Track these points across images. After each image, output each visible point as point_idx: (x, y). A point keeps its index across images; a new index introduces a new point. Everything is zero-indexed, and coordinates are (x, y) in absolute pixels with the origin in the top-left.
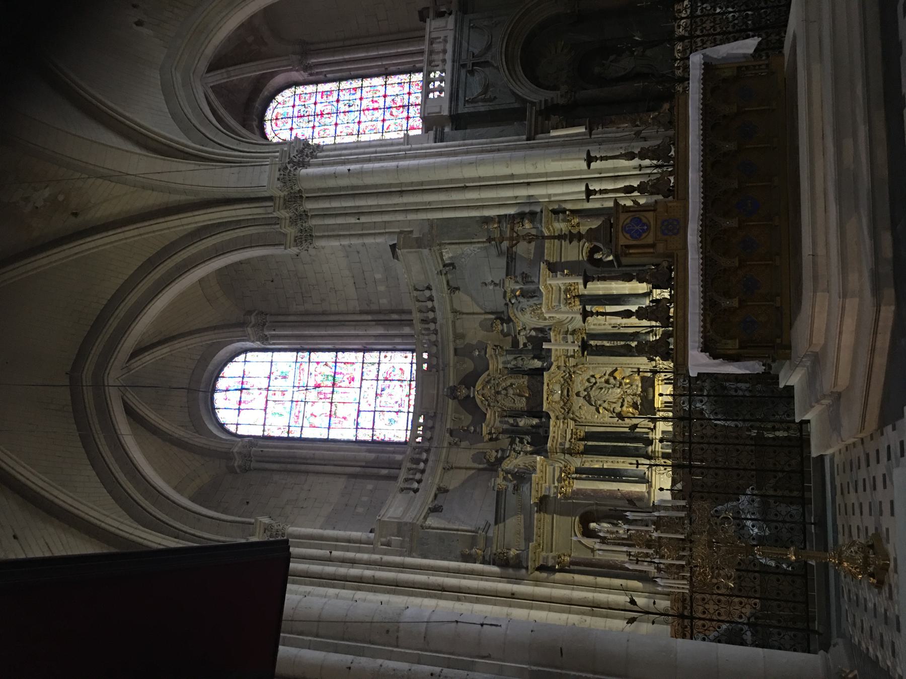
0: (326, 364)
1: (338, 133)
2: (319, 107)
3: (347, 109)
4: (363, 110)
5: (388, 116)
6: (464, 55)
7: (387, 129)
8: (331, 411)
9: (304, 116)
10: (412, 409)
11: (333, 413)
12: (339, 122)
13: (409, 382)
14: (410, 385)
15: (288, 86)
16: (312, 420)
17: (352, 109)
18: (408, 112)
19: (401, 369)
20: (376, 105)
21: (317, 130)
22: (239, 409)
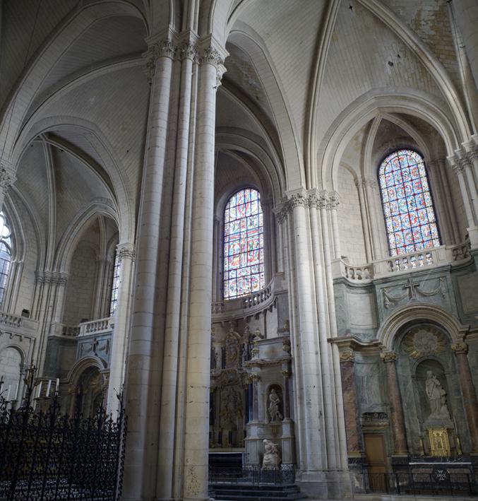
1: (392, 203)
3: (409, 203)
6: (415, 280)
12: (399, 201)
16: (232, 246)
17: (410, 206)
20: (413, 222)
21: (393, 188)
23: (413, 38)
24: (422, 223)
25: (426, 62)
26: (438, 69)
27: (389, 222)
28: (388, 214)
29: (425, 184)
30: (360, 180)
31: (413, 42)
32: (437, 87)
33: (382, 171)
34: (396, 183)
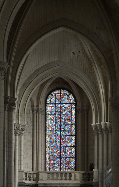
2: (64, 116)
4: (61, 137)
5: (57, 149)
7: (51, 149)
9: (61, 109)
15: (75, 100)
18: (58, 158)
20: (62, 143)
23: (90, 52)
24: (68, 145)
25: (94, 67)
26: (99, 74)
27: (48, 139)
28: (48, 133)
29: (73, 119)
30: (35, 108)
31: (90, 53)
32: (95, 78)
33: (48, 101)
34: (56, 113)
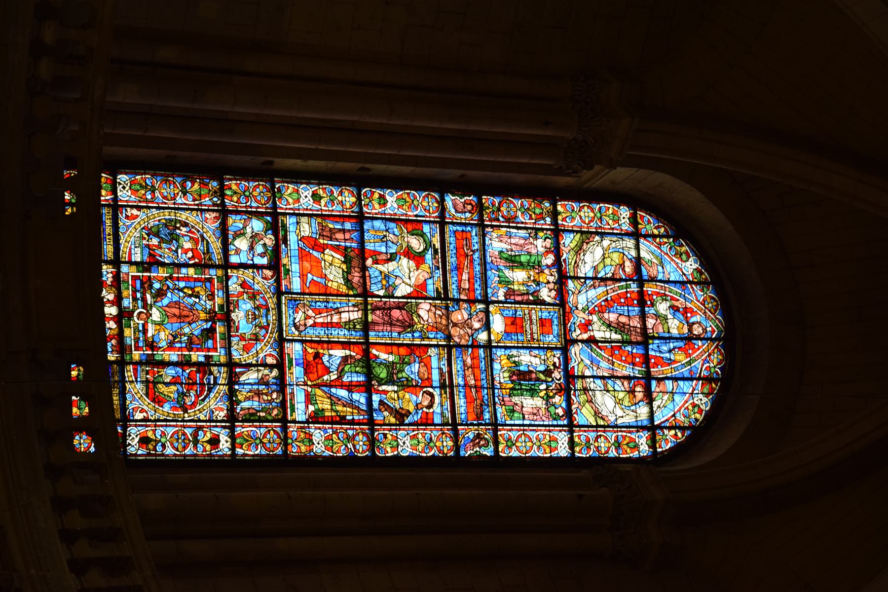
0: (401, 415)
8: (364, 269)
10: (107, 272)
11: (355, 262)
13: (128, 358)
14: (122, 348)
16: (417, 244)
19: (158, 400)
22: (641, 282)
